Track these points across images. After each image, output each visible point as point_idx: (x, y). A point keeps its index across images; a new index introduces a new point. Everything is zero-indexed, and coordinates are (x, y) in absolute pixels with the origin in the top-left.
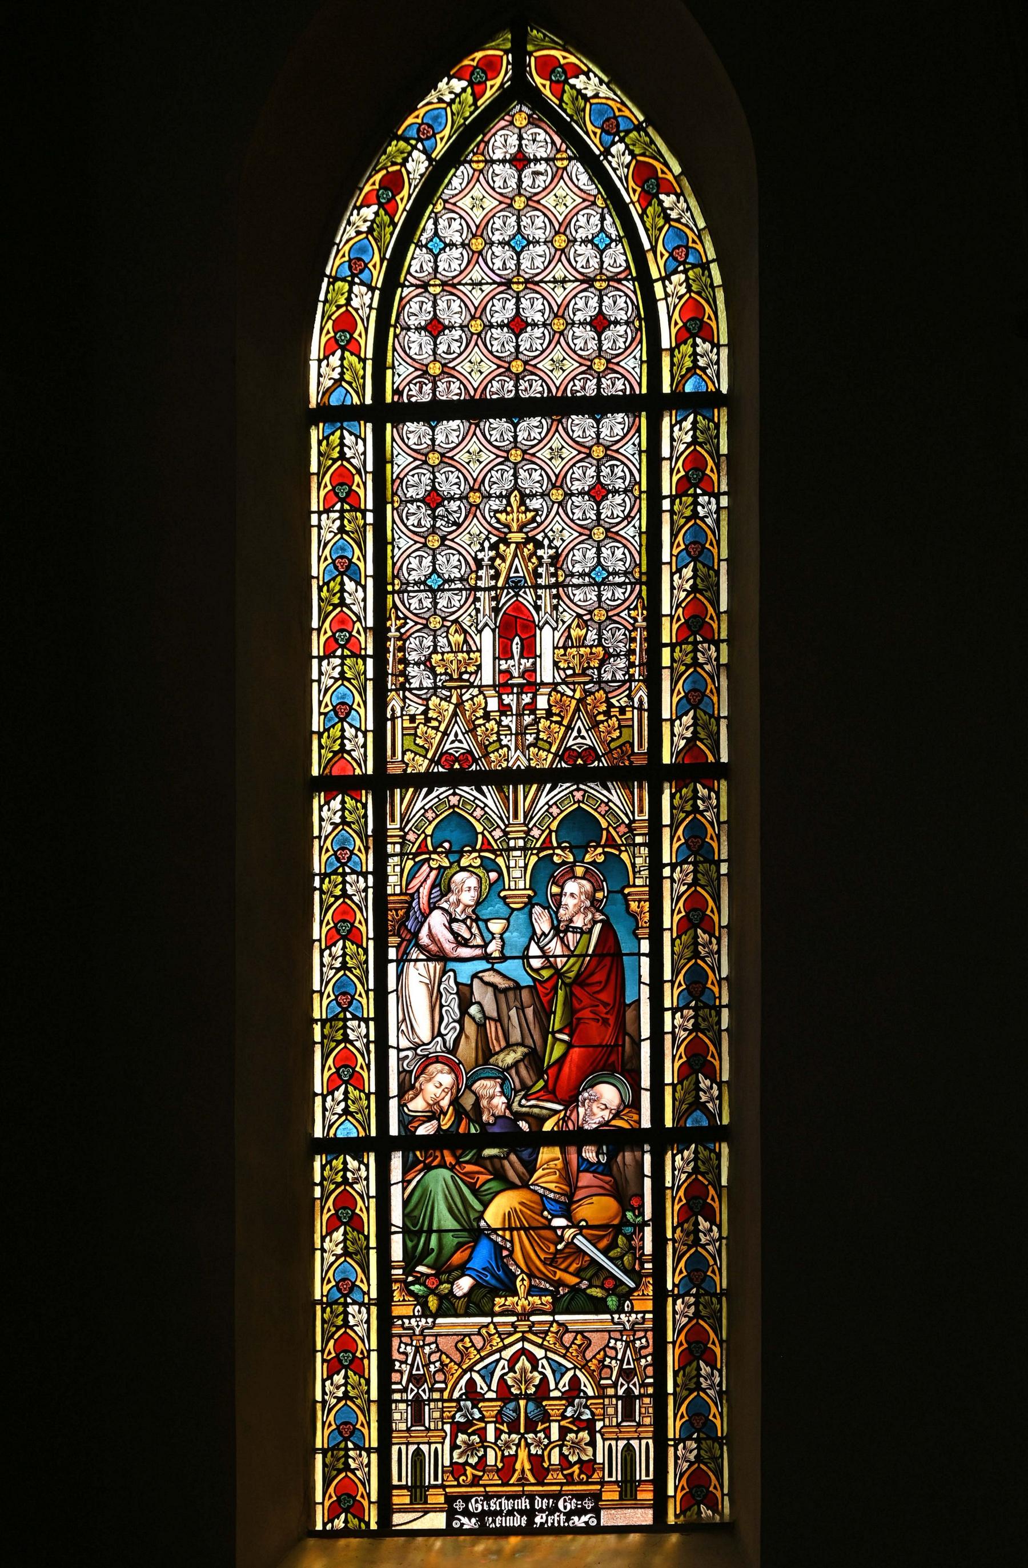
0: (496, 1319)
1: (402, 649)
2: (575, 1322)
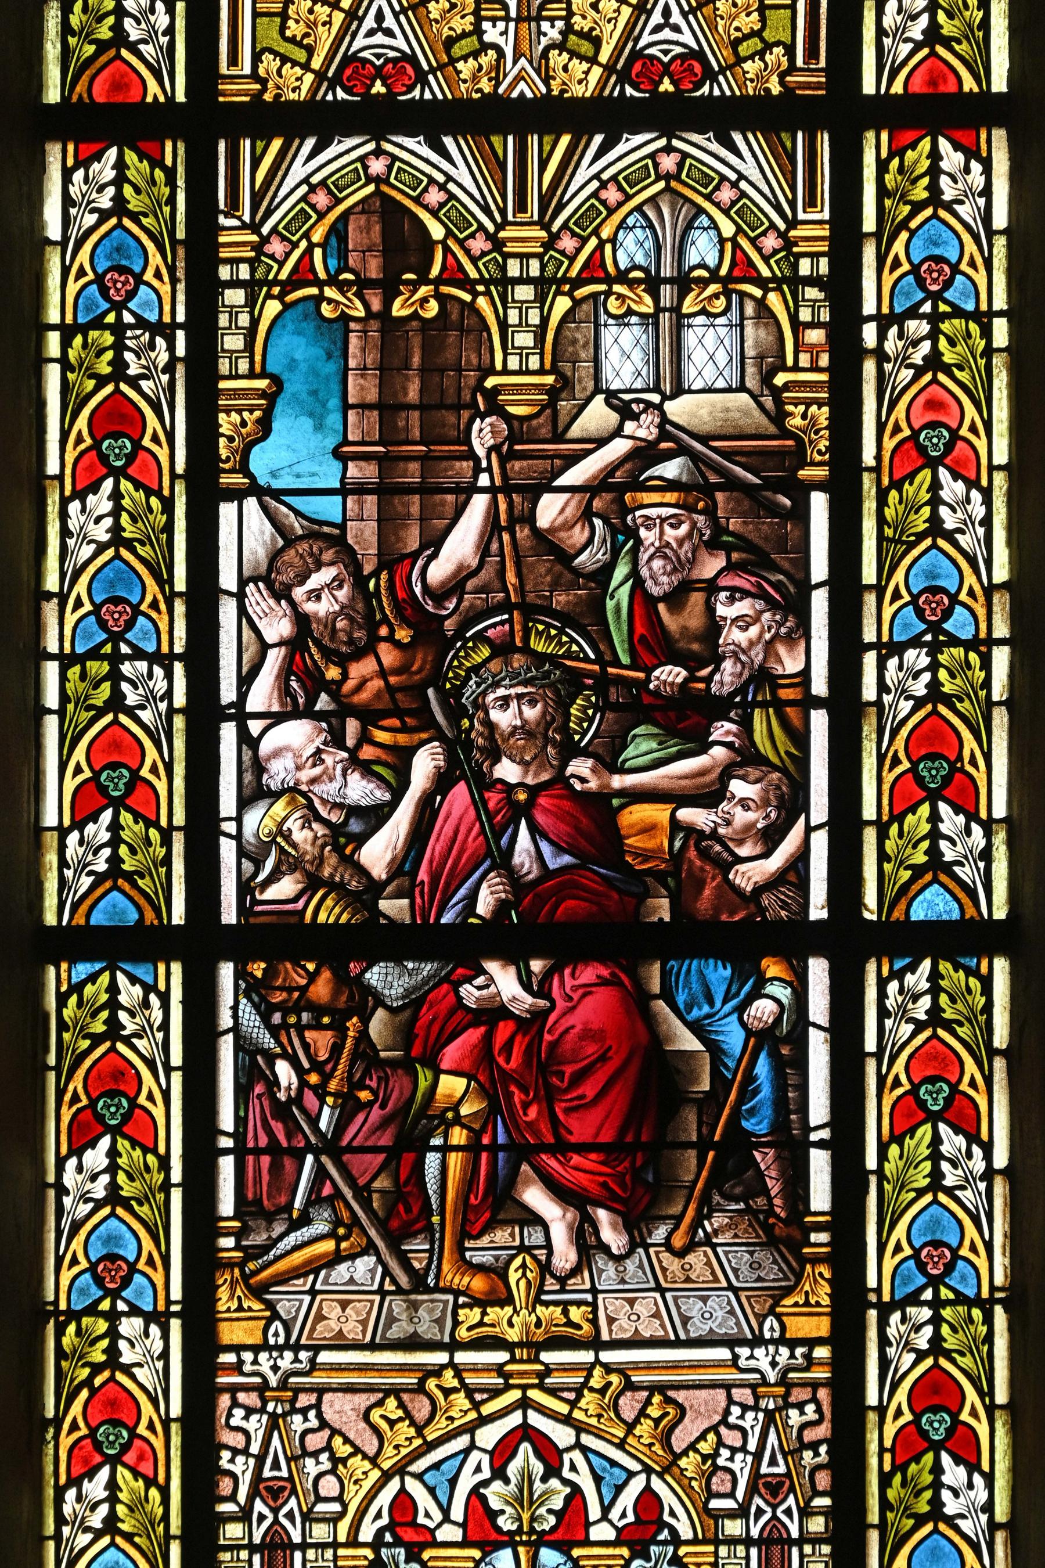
0: (461, 1357)
2: (649, 1366)
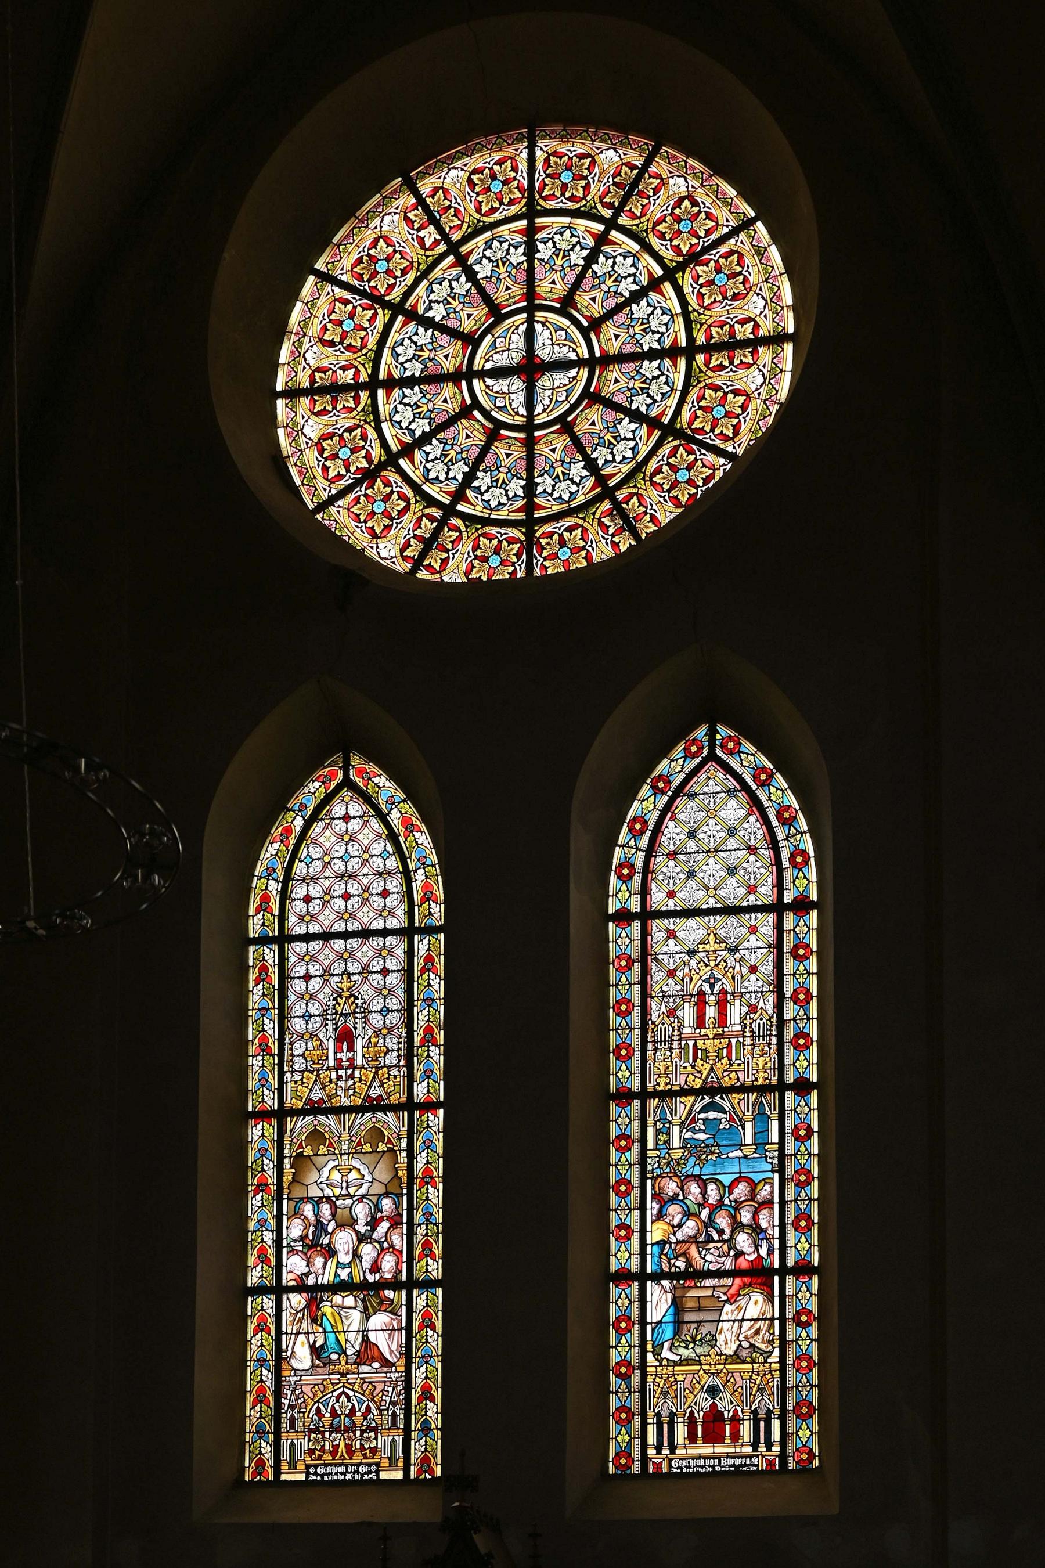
1: (291, 1049)
